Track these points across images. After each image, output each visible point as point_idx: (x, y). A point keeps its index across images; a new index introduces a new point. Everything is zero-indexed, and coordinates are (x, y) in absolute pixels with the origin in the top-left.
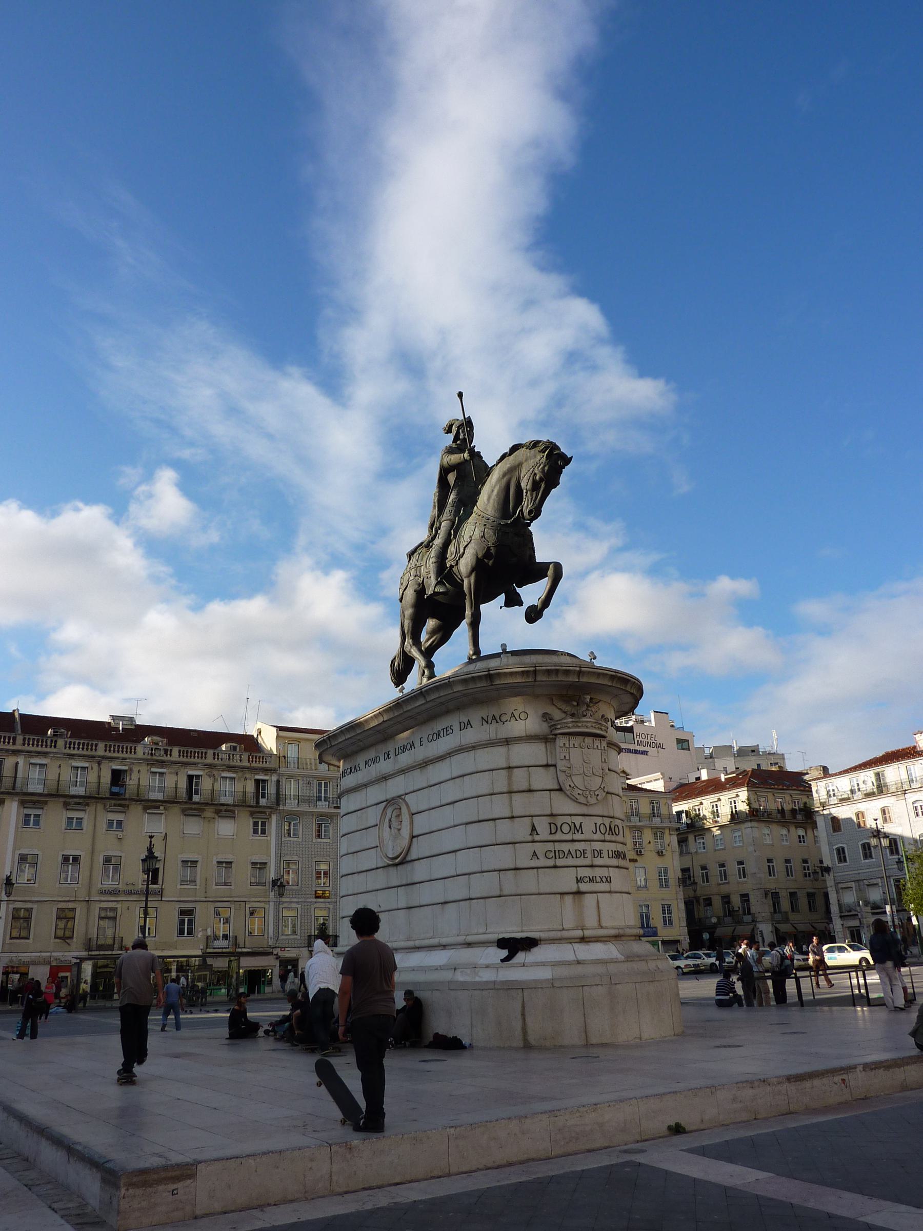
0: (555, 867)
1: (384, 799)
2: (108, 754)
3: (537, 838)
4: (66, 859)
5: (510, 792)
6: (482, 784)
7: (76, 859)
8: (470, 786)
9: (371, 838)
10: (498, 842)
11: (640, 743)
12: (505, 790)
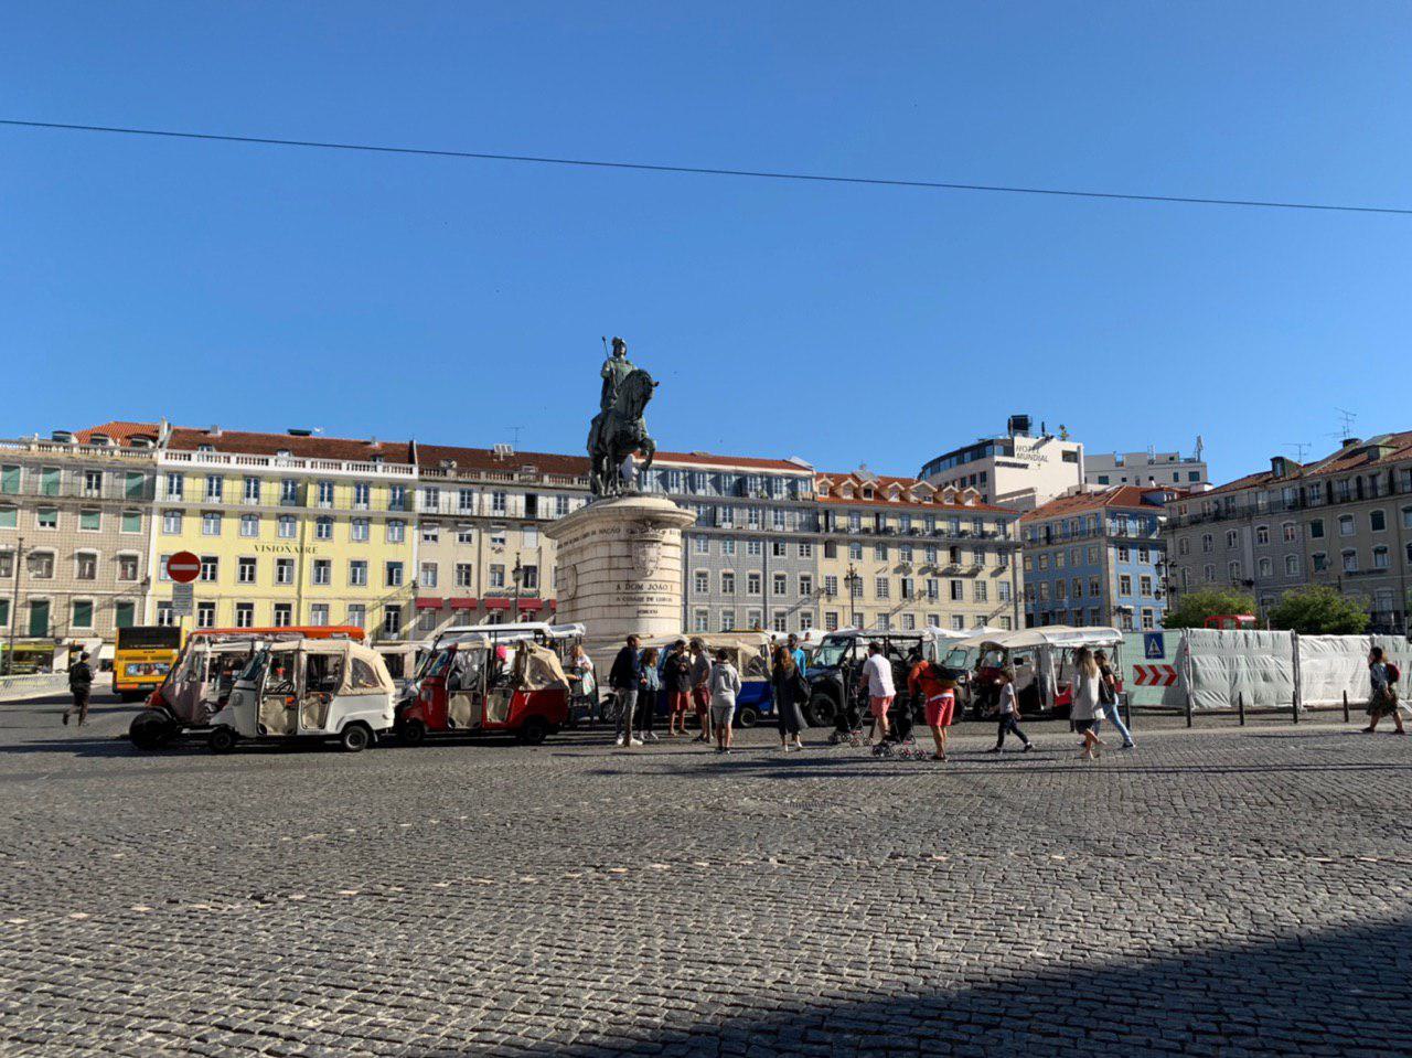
2: (489, 481)
4: (460, 566)
5: (610, 569)
7: (469, 567)
11: (1019, 457)
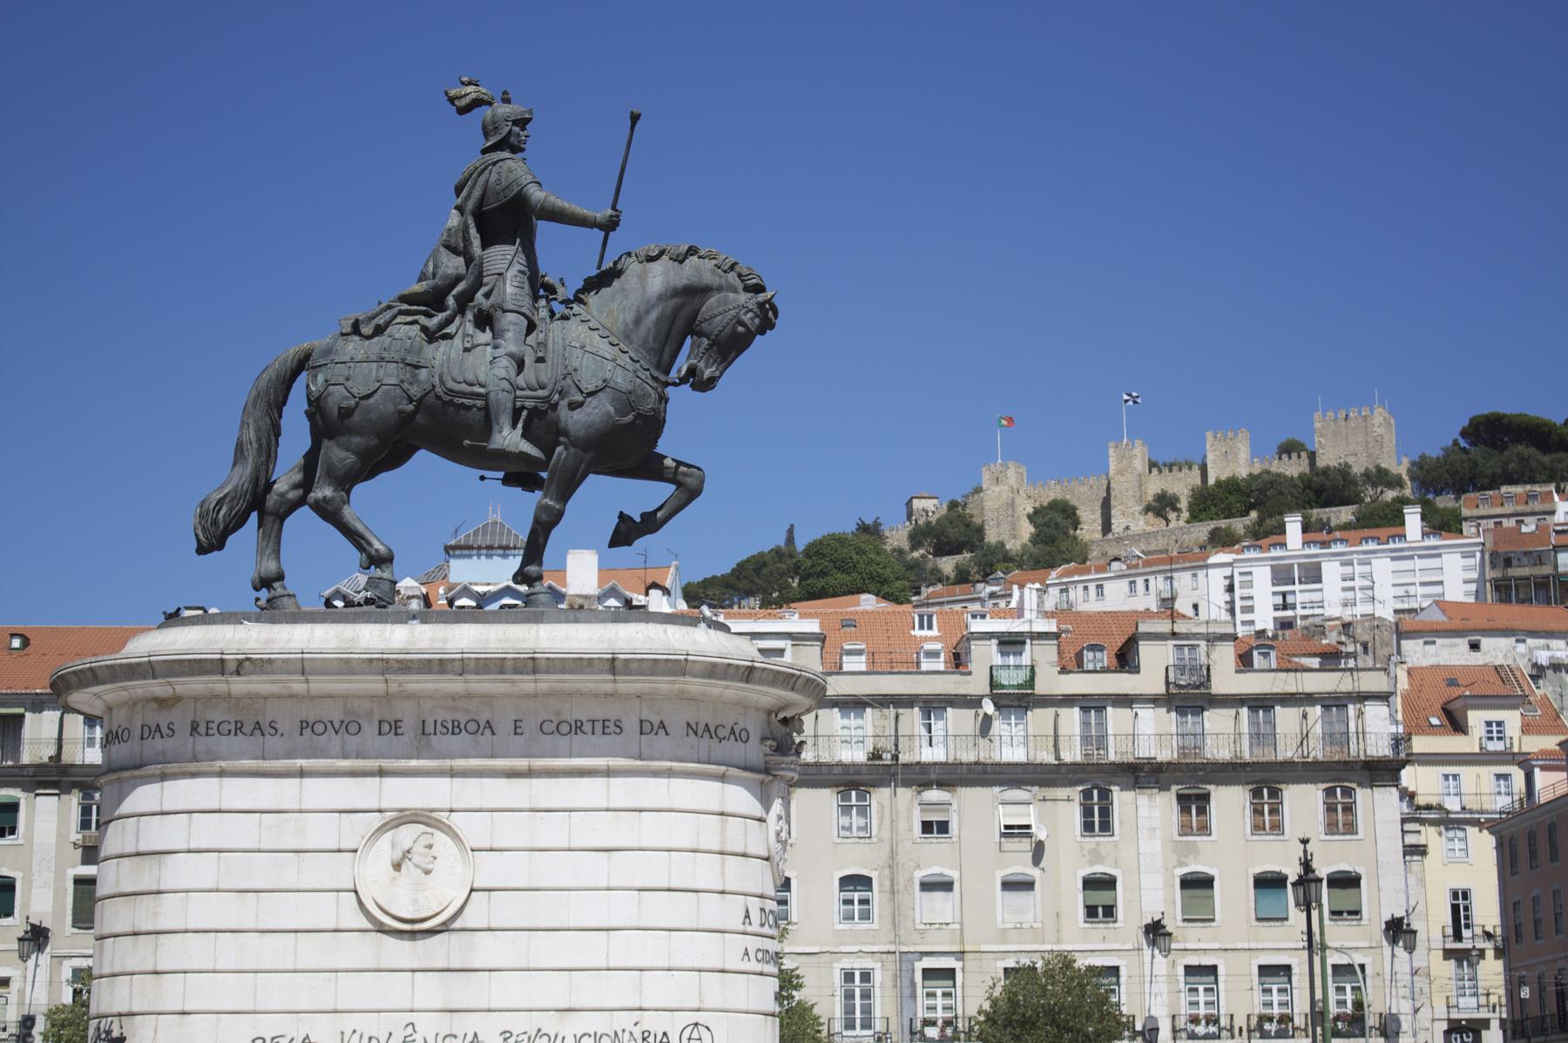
0: (761, 974)
1: (375, 806)
3: (749, 929)
6: (681, 831)
8: (652, 830)
9: (337, 871)
10: (701, 926)
12: (717, 848)
